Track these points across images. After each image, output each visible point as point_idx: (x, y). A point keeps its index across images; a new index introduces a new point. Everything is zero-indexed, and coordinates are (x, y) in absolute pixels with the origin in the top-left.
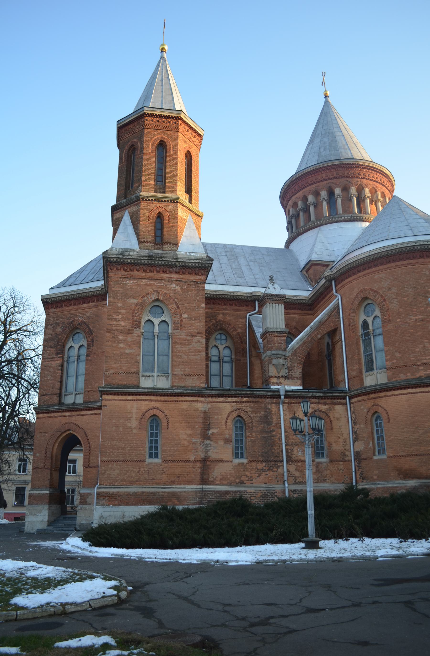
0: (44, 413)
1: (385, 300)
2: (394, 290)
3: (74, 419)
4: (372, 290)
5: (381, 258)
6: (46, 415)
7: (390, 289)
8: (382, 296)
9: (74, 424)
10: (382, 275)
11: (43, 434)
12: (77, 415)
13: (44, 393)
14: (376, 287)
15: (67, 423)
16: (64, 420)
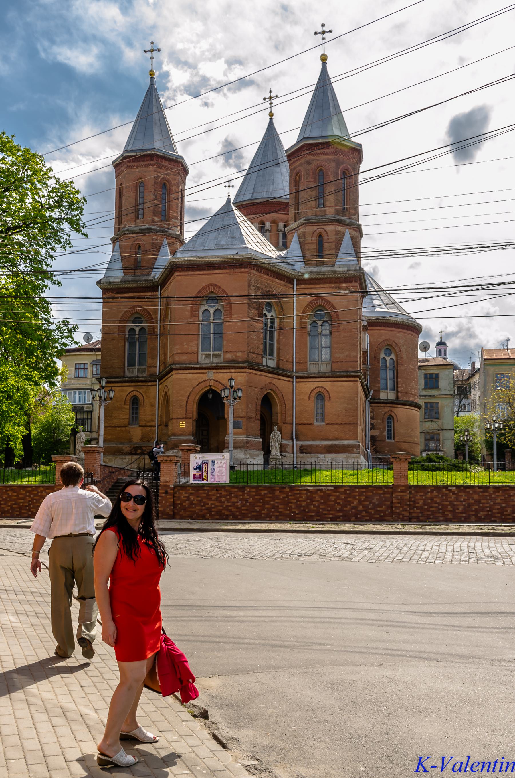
0: (252, 369)
1: (400, 351)
2: (405, 347)
3: (274, 381)
4: (394, 341)
5: (402, 325)
6: (254, 372)
7: (403, 346)
8: (399, 348)
9: (275, 385)
10: (400, 335)
11: (253, 389)
12: (277, 379)
13: (252, 351)
14: (397, 341)
15: (270, 383)
16: (268, 380)
